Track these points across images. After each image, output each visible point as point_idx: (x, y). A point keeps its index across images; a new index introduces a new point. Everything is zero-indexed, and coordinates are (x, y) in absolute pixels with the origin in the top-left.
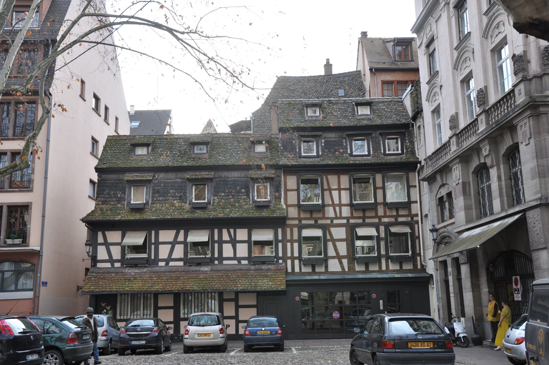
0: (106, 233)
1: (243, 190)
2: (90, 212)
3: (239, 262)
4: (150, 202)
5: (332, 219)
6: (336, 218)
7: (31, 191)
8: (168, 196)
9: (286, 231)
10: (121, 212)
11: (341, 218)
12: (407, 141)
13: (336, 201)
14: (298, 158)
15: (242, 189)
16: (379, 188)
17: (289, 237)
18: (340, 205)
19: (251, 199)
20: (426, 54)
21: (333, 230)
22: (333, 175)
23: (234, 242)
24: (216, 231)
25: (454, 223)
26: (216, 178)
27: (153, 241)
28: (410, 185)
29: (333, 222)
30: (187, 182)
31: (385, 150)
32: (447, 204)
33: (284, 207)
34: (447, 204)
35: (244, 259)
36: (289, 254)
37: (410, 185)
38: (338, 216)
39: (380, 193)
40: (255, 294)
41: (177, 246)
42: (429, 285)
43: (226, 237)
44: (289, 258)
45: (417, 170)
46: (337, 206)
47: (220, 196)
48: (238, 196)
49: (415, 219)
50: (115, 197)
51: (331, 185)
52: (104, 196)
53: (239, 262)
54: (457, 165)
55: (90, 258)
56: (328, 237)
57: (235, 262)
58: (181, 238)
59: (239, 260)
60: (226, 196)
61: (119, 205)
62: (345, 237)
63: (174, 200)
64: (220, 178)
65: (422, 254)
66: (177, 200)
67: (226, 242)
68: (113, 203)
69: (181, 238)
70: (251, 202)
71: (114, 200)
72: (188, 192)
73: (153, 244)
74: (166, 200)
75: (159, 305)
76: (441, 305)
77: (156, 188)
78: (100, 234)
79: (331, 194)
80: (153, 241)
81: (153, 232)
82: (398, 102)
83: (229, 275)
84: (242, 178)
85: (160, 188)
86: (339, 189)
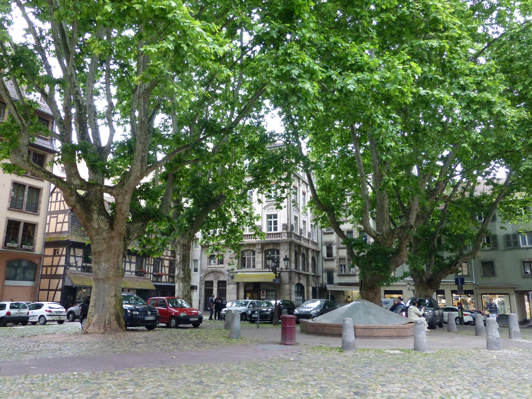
5: (165, 256)
6: (166, 256)
7: (38, 215)
11: (168, 256)
35: (133, 272)
40: (135, 291)
57: (130, 273)
59: (132, 272)
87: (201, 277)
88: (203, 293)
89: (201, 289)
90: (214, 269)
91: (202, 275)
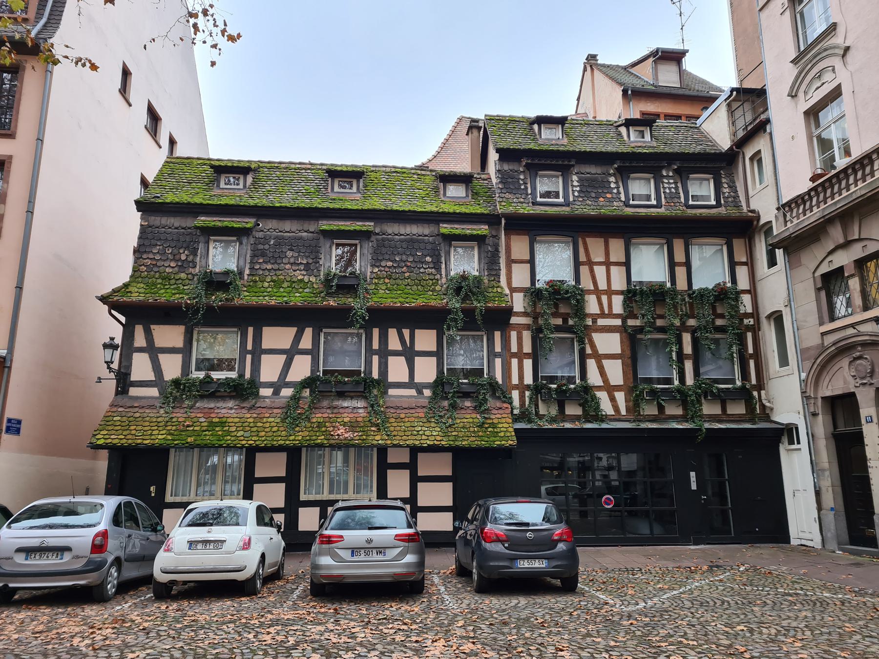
0: (152, 327)
1: (428, 259)
2: (120, 284)
3: (420, 392)
4: (247, 272)
5: (595, 318)
6: (603, 315)
8: (282, 263)
9: (510, 336)
10: (185, 288)
11: (611, 315)
12: (726, 186)
13: (602, 285)
14: (531, 204)
15: (426, 256)
16: (680, 264)
17: (514, 349)
18: (610, 292)
19: (444, 276)
20: (788, 10)
21: (596, 337)
22: (596, 237)
23: (410, 354)
24: (376, 332)
26: (378, 234)
27: (249, 347)
28: (736, 260)
29: (596, 322)
30: (322, 238)
31: (686, 199)
32: (854, 284)
33: (507, 291)
34: (854, 284)
36: (515, 380)
37: (736, 260)
38: (606, 312)
39: (681, 272)
41: (297, 358)
42: (780, 445)
43: (394, 343)
44: (516, 387)
46: (604, 294)
47: (384, 267)
48: (420, 268)
50: (174, 260)
51: (592, 256)
52: (151, 256)
53: (420, 392)
55: (112, 375)
56: (589, 351)
57: (413, 392)
58: (306, 342)
59: (419, 388)
60: (395, 267)
61: (183, 275)
62: (618, 351)
63: (295, 271)
64: (384, 234)
66: (300, 270)
67: (396, 353)
68: (171, 271)
69: (306, 342)
70: (444, 280)
71: (173, 264)
72: (322, 256)
73: (249, 352)
74: (279, 269)
75: (257, 475)
76: (827, 483)
77: (261, 247)
78: (139, 331)
79: (592, 272)
80: (249, 347)
81: (251, 330)
82: (691, 127)
83: (402, 416)
84: (426, 236)
85: (267, 247)
86: (608, 264)
87: (804, 383)
88: (825, 457)
89: (812, 437)
90: (851, 331)
91: (803, 375)
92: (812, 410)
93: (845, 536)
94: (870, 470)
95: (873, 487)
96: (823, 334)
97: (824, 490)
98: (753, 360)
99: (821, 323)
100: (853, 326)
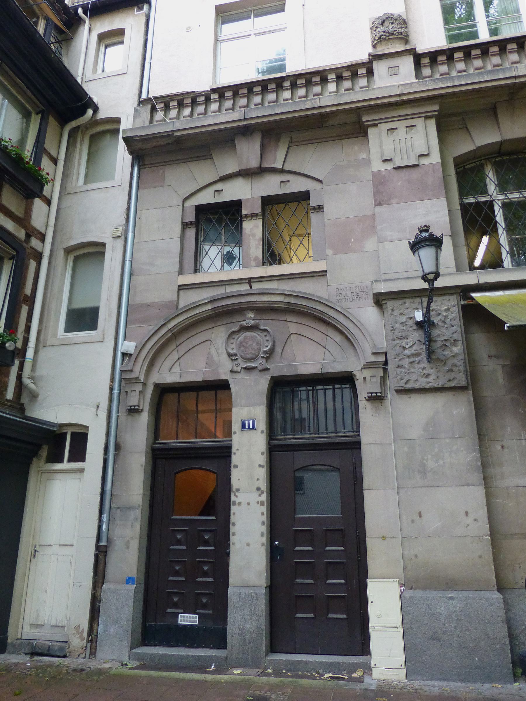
25: (323, 274)
45: (74, 124)
49: (35, 243)
54: (420, 122)
65: (30, 354)
90: (245, 288)
92: (133, 401)
93: (139, 636)
94: (233, 509)
95: (233, 539)
96: (182, 288)
97: (118, 545)
98: (27, 308)
99: (181, 272)
100: (250, 281)
